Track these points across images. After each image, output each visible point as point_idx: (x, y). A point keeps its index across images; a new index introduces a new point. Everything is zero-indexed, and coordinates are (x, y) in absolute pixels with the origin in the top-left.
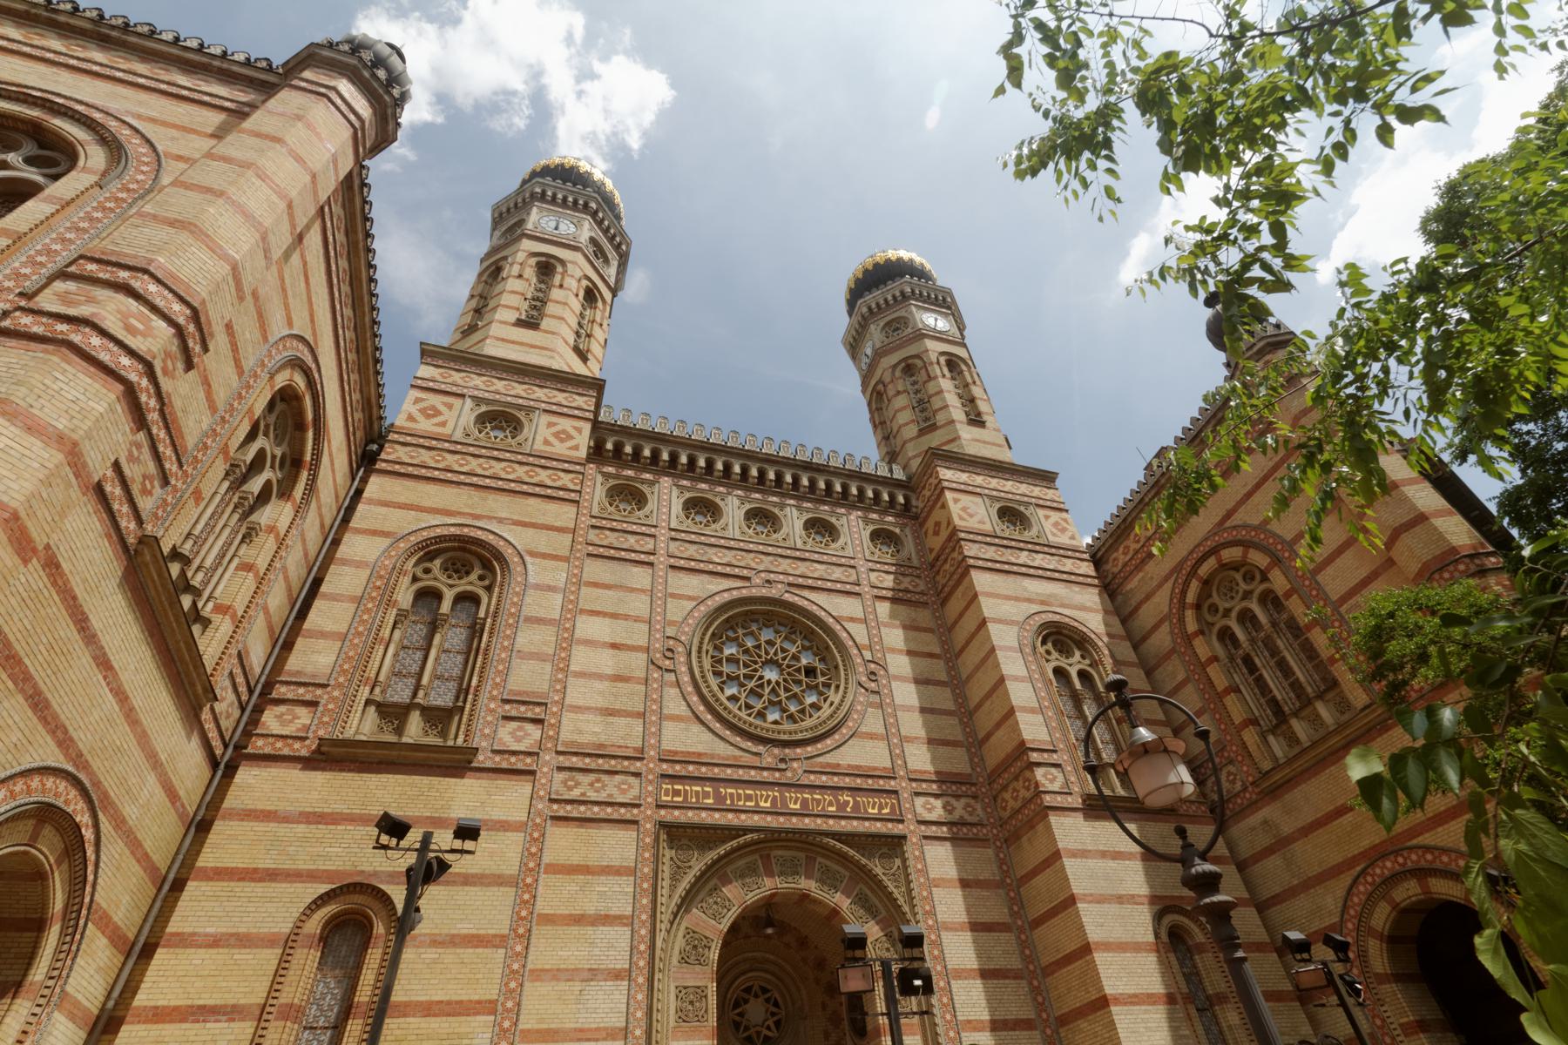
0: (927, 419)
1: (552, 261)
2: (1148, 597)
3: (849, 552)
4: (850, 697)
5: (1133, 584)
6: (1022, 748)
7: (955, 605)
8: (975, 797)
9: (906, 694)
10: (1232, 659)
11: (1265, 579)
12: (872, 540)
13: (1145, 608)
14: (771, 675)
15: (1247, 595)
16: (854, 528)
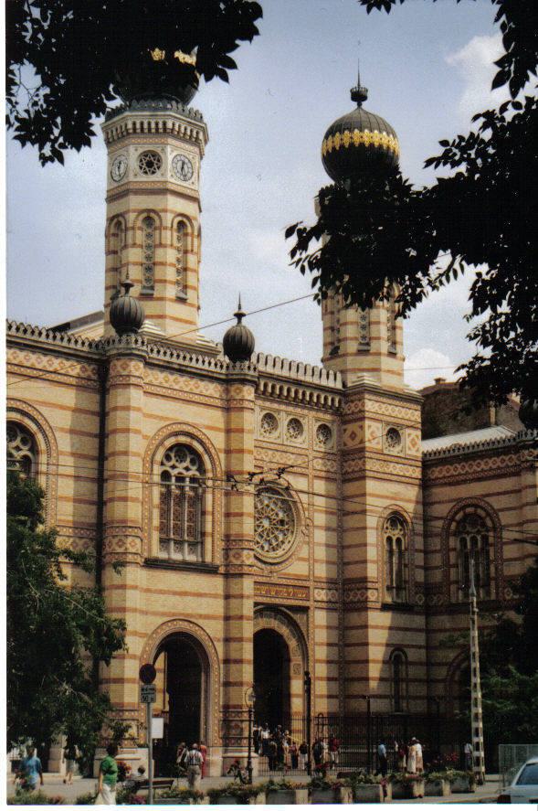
0: (364, 337)
1: (185, 220)
2: (439, 503)
3: (304, 446)
4: (298, 539)
5: (436, 491)
6: (364, 580)
7: (351, 488)
8: (336, 590)
9: (320, 536)
10: (461, 550)
11: (488, 531)
12: (318, 430)
13: (436, 506)
14: (266, 523)
15: (478, 532)
16: (311, 420)
